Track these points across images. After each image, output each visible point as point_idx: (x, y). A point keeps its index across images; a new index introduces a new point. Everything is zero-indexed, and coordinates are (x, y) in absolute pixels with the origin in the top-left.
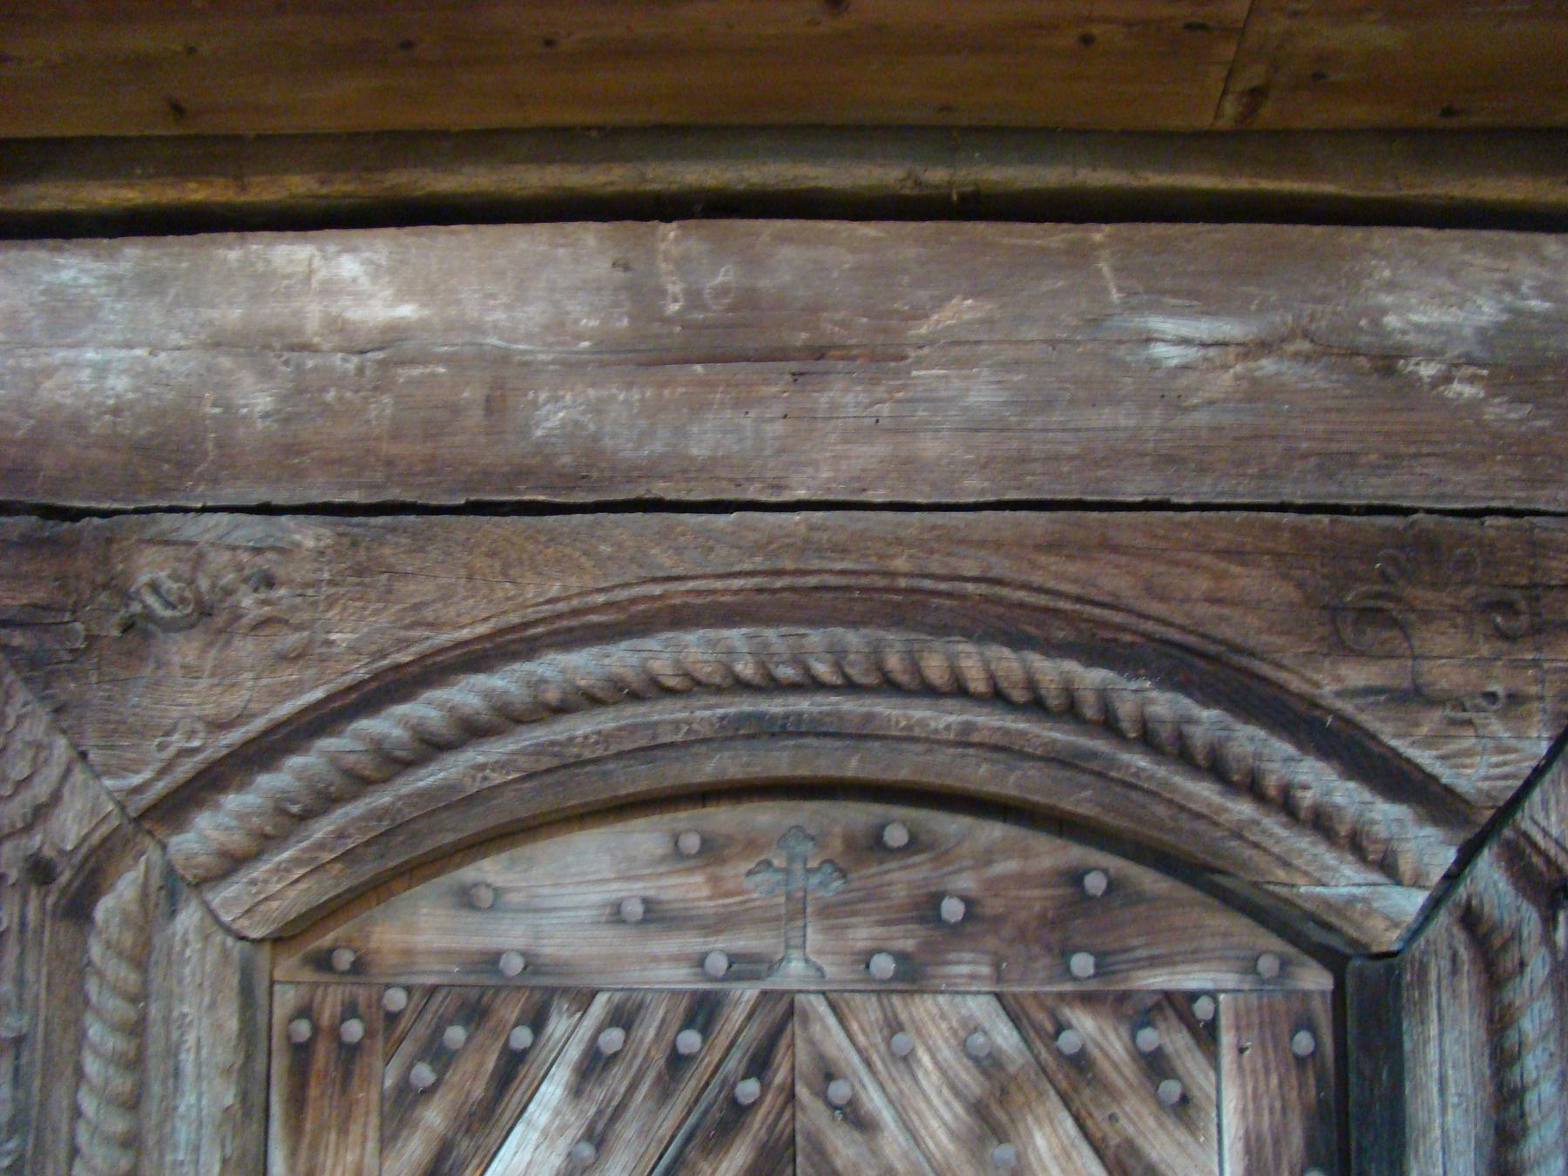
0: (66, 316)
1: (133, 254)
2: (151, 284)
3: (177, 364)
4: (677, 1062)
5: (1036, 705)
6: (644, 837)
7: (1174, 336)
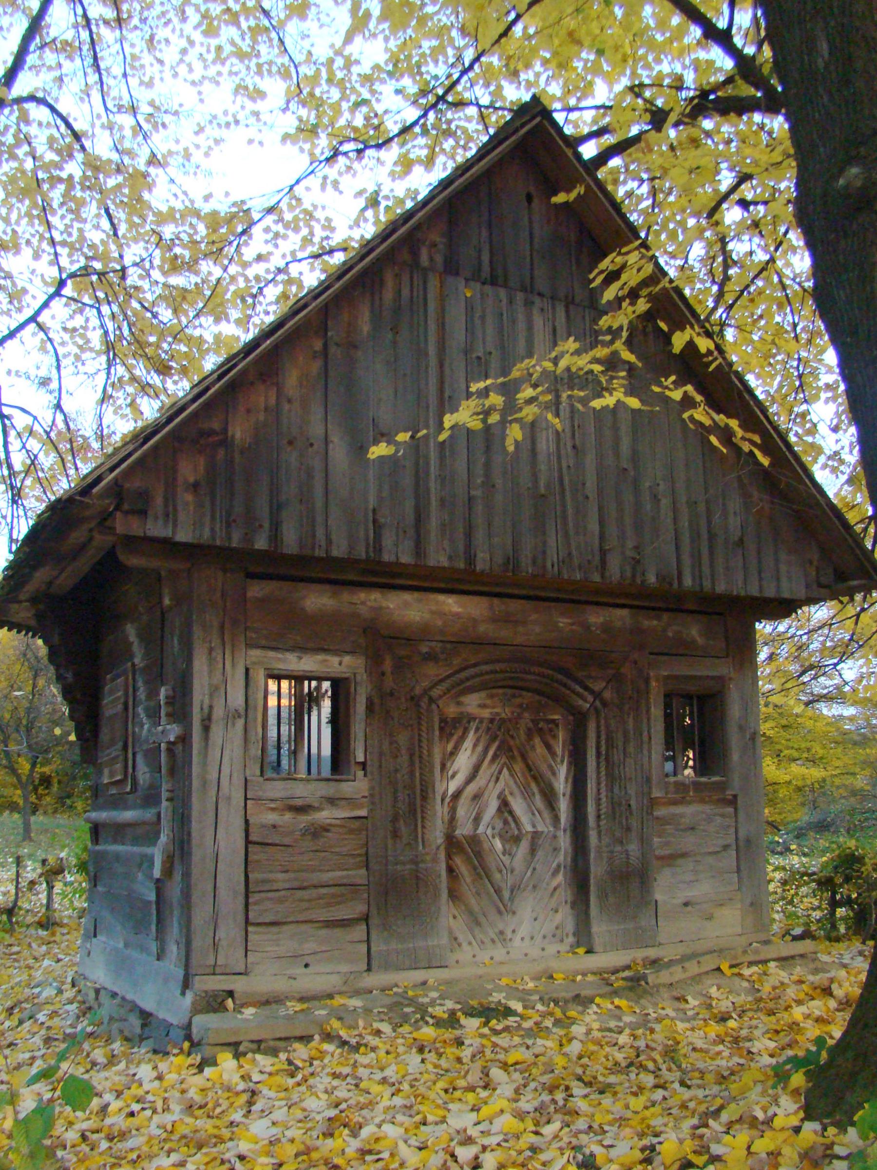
0: (407, 604)
1: (416, 595)
2: (420, 601)
3: (427, 616)
4: (489, 729)
5: (543, 676)
6: (483, 694)
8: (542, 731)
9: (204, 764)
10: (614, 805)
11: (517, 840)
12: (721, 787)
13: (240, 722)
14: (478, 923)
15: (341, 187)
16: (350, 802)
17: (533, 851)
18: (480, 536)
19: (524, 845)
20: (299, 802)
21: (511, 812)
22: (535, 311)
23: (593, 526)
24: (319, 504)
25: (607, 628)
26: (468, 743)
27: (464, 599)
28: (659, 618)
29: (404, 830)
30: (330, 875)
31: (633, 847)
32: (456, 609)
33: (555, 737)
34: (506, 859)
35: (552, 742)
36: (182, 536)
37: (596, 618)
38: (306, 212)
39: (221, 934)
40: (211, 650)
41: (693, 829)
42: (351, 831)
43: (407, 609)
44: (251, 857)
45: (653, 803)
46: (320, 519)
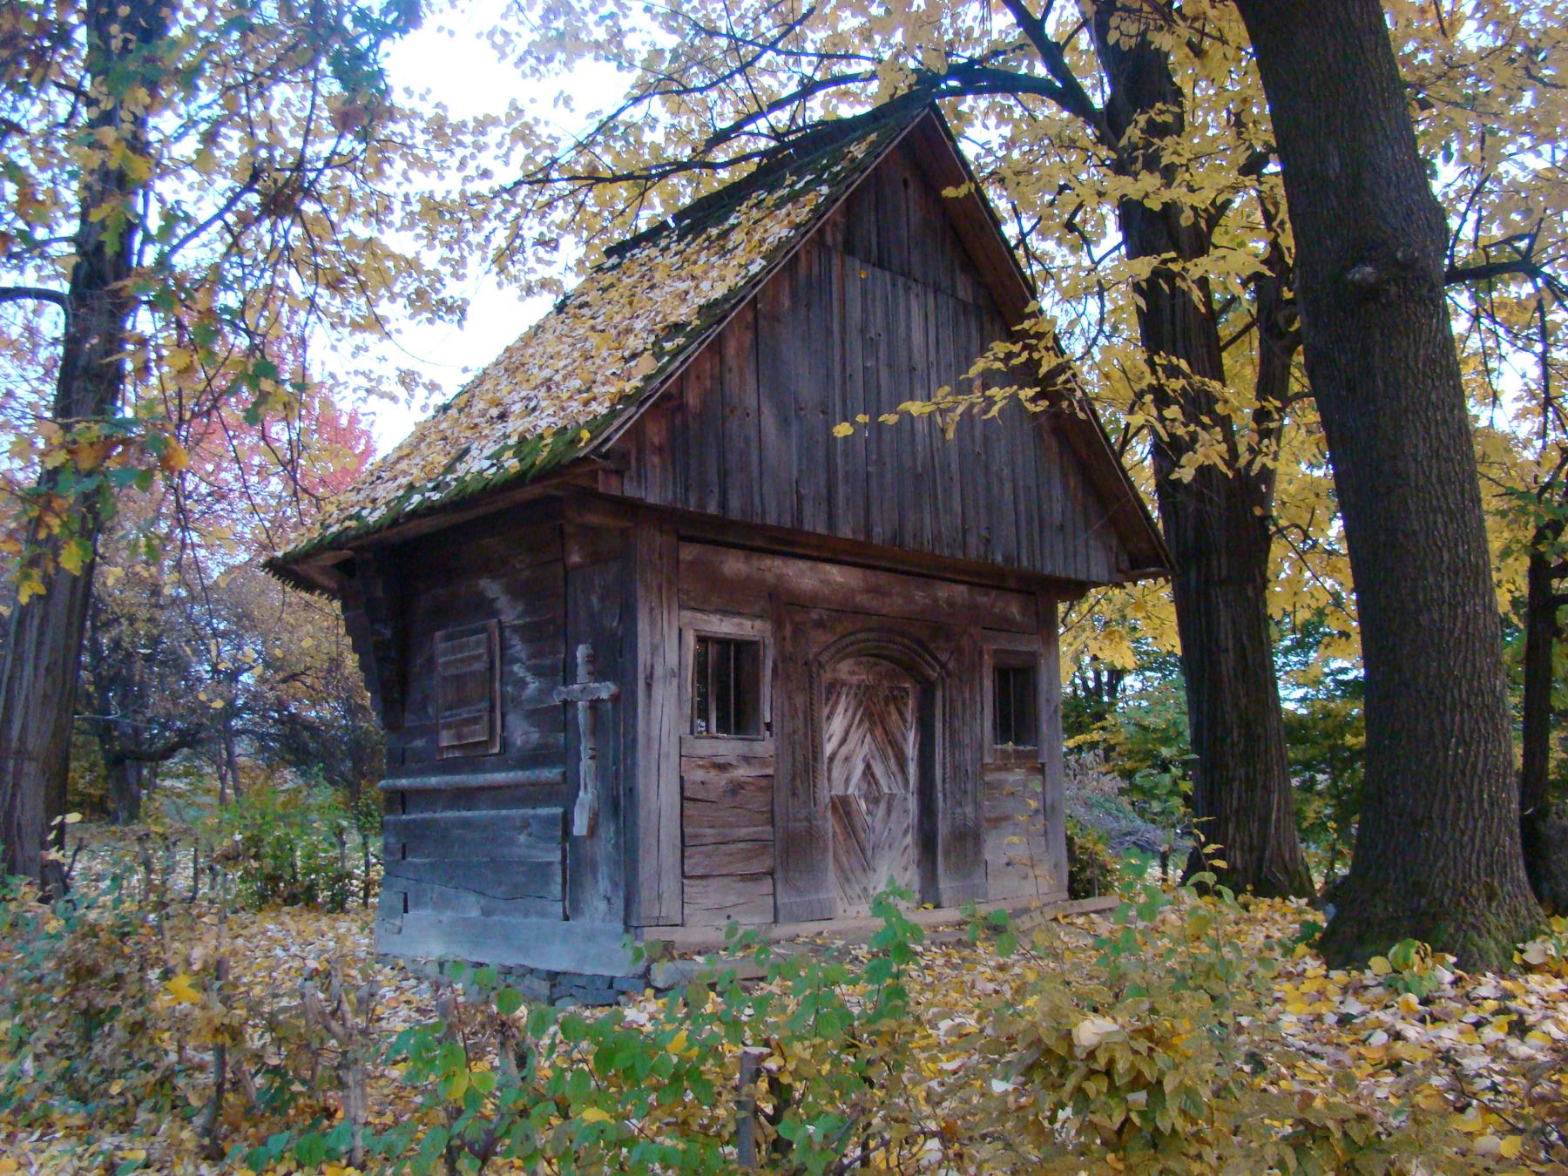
6: (852, 661)
8: (896, 698)
9: (648, 723)
10: (956, 768)
11: (876, 801)
12: (1035, 755)
13: (675, 682)
14: (848, 880)
15: (573, 104)
16: (762, 762)
17: (889, 811)
18: (875, 509)
19: (883, 806)
20: (721, 760)
21: (873, 775)
22: (912, 296)
23: (957, 507)
24: (756, 474)
27: (845, 568)
28: (987, 594)
29: (801, 791)
31: (969, 810)
32: (839, 579)
33: (906, 704)
34: (869, 819)
36: (653, 498)
37: (943, 592)
38: (526, 125)
39: (664, 886)
40: (651, 609)
42: (761, 789)
43: (803, 576)
44: (686, 812)
45: (984, 768)
46: (756, 488)
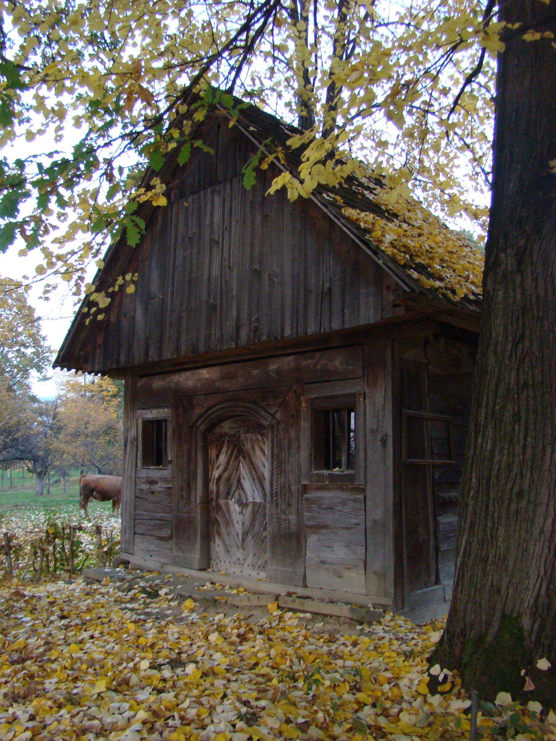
1: (192, 372)
6: (230, 420)
7: (255, 372)
12: (351, 478)
19: (250, 508)
21: (243, 489)
25: (278, 372)
26: (224, 449)
28: (312, 358)
30: (160, 515)
31: (293, 518)
35: (263, 447)
37: (273, 366)
41: (331, 509)
43: (187, 380)
45: (305, 489)
